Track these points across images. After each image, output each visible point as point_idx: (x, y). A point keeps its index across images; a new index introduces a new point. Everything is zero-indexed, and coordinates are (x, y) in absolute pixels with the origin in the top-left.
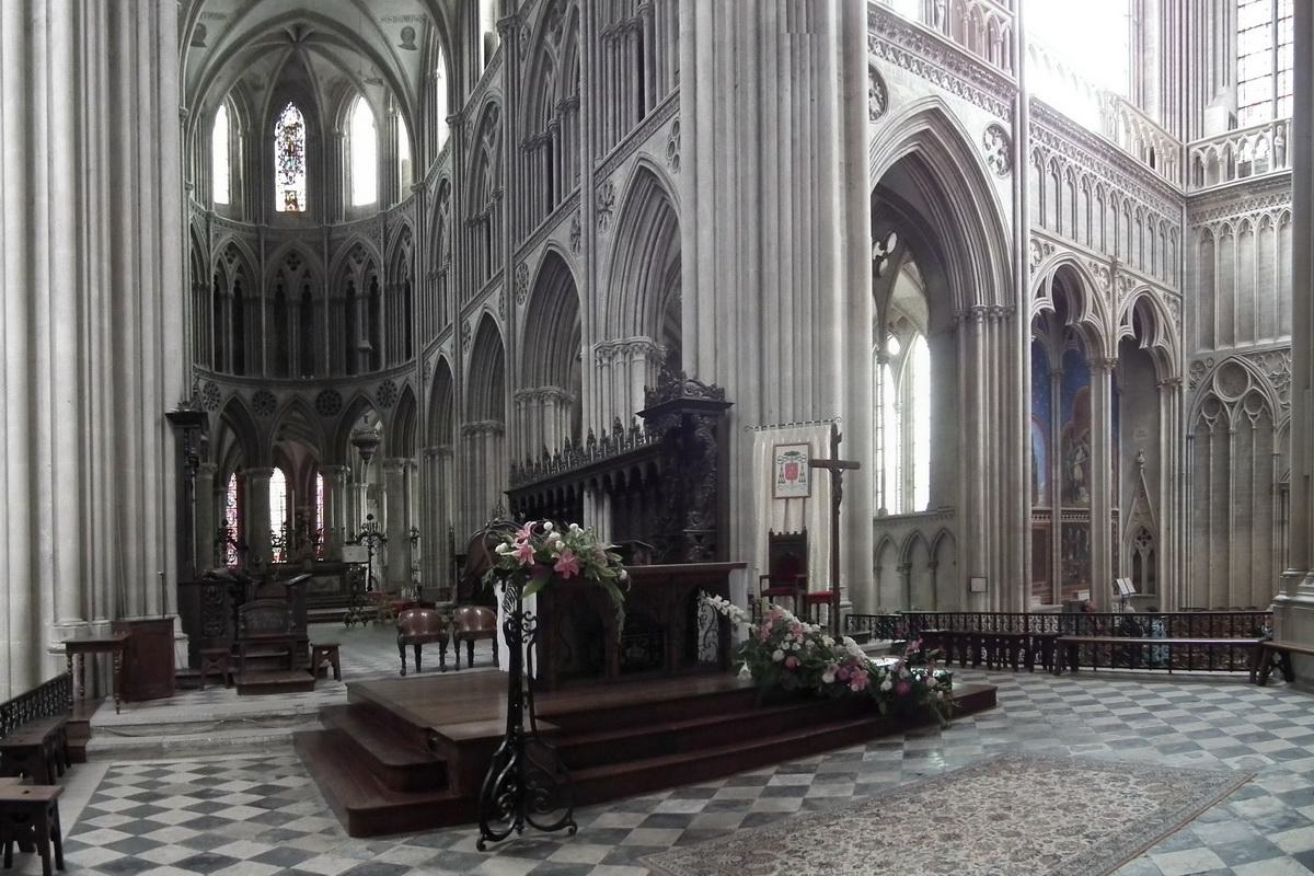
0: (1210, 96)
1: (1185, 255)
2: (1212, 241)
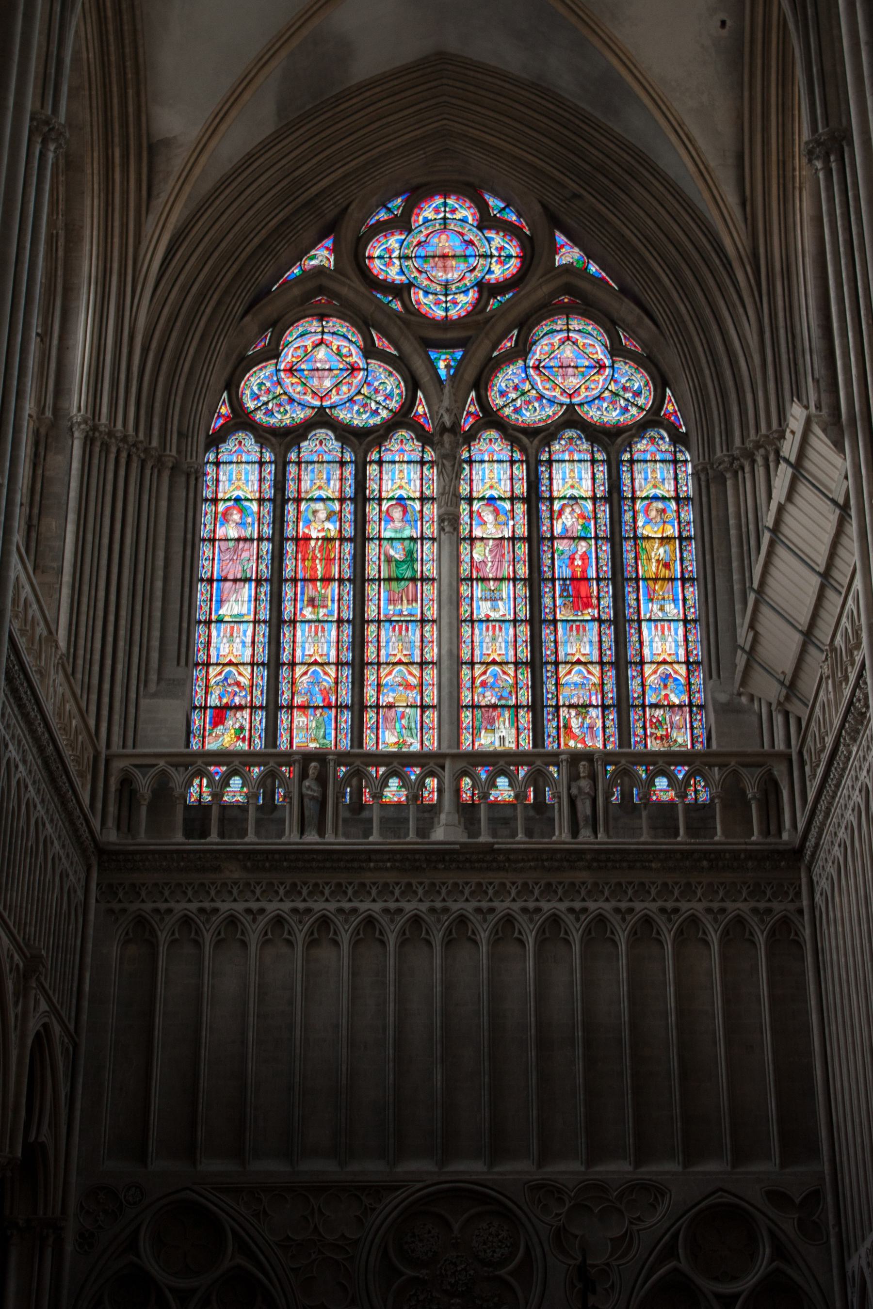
0: (153, 677)
1: (88, 960)
2: (153, 946)
